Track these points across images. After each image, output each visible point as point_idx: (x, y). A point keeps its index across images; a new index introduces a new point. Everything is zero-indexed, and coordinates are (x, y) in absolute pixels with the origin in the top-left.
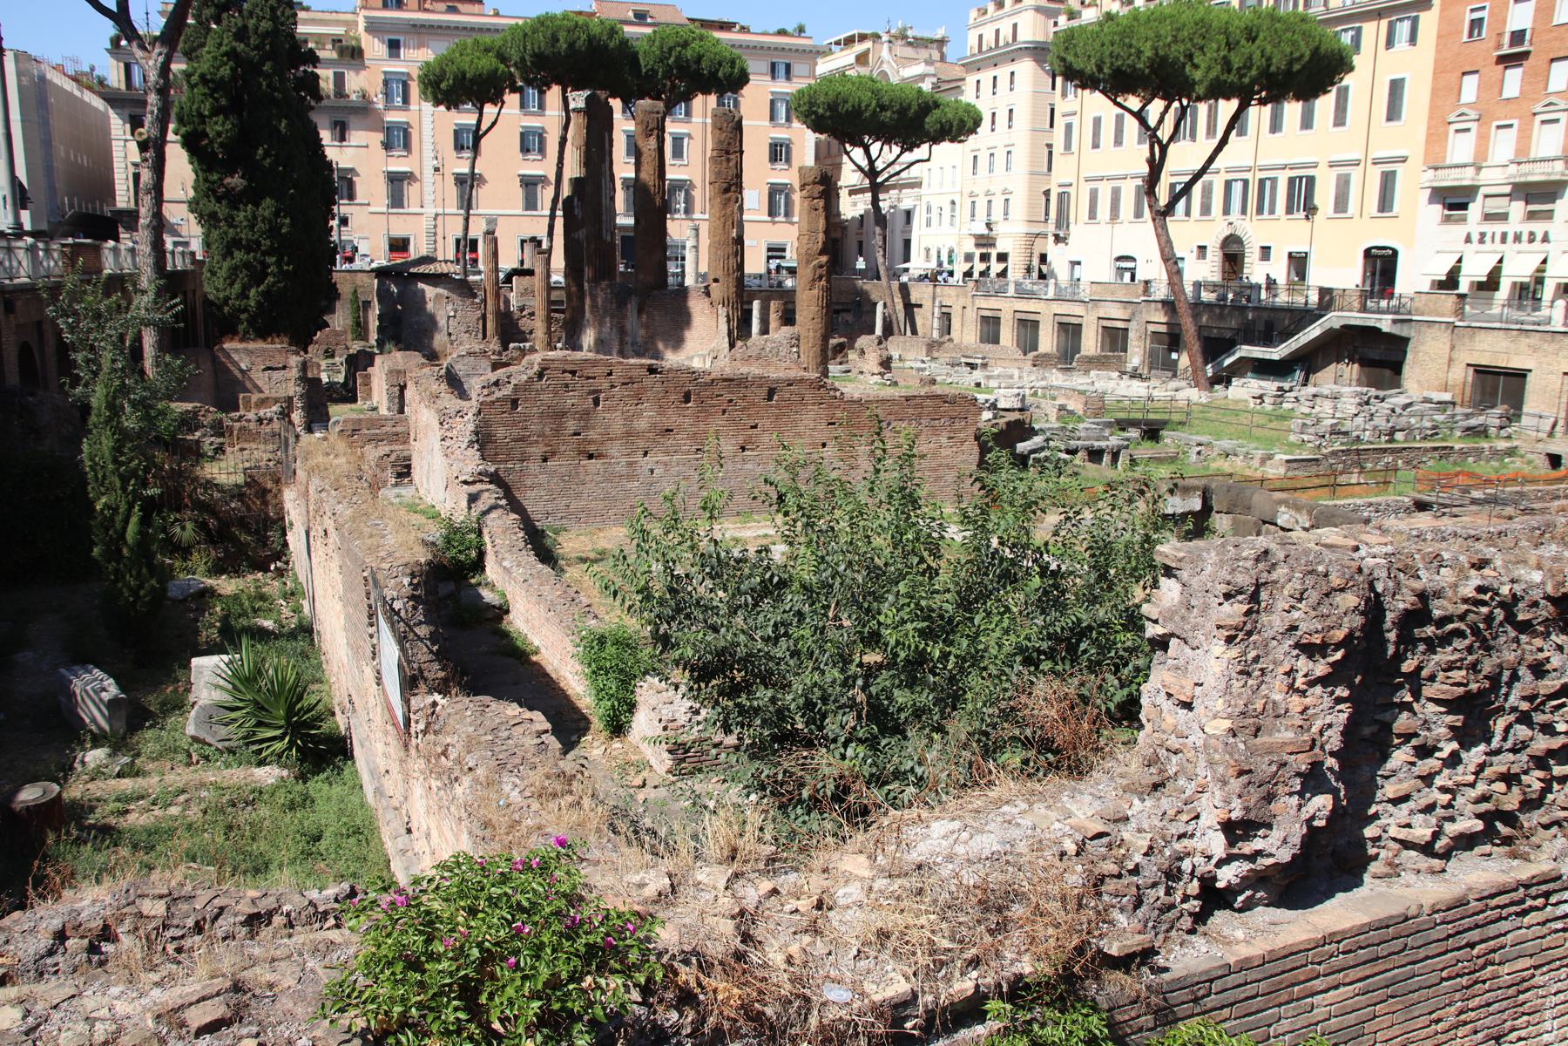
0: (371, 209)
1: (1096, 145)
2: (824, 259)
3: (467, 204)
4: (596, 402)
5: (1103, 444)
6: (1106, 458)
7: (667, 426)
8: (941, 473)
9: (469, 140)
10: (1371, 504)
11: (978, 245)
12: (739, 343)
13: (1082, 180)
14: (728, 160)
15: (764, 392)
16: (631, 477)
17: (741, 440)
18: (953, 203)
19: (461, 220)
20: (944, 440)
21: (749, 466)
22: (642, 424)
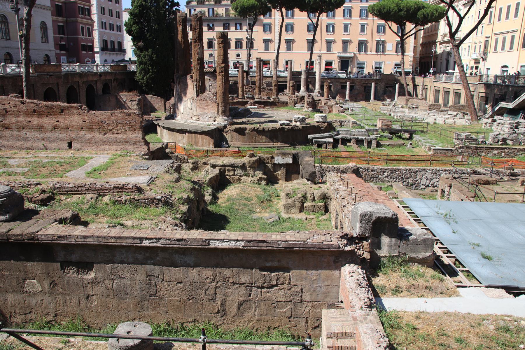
0: (258, 51)
1: (499, 20)
2: (223, 65)
3: (311, 49)
4: (7, 112)
5: (363, 138)
6: (365, 144)
7: (29, 120)
8: (127, 140)
9: (312, 28)
10: (446, 170)
11: (475, 63)
12: (200, 95)
13: (493, 35)
14: (196, 32)
15: (59, 110)
16: (20, 135)
17: (53, 125)
18: (469, 46)
19: (310, 54)
20: (127, 129)
21: (57, 134)
22: (21, 119)
